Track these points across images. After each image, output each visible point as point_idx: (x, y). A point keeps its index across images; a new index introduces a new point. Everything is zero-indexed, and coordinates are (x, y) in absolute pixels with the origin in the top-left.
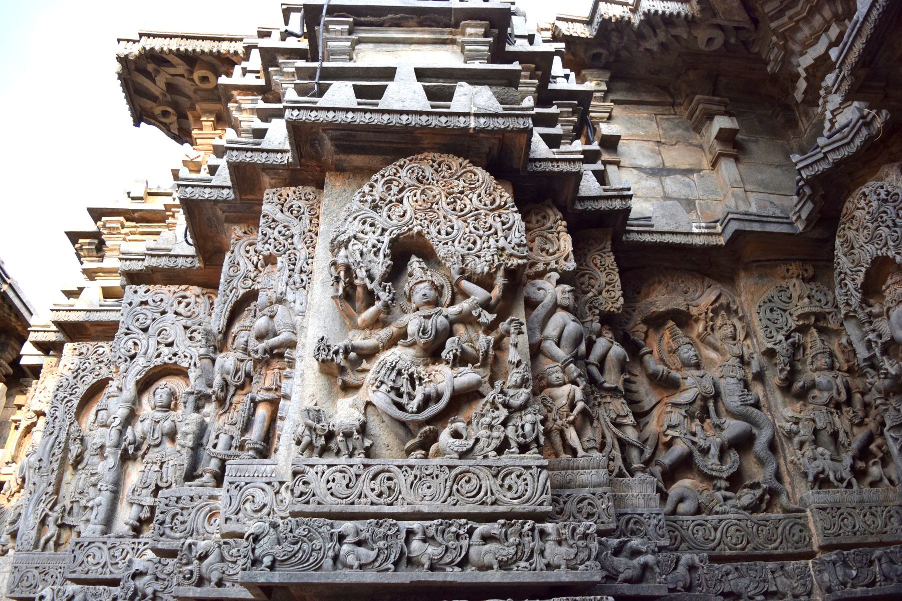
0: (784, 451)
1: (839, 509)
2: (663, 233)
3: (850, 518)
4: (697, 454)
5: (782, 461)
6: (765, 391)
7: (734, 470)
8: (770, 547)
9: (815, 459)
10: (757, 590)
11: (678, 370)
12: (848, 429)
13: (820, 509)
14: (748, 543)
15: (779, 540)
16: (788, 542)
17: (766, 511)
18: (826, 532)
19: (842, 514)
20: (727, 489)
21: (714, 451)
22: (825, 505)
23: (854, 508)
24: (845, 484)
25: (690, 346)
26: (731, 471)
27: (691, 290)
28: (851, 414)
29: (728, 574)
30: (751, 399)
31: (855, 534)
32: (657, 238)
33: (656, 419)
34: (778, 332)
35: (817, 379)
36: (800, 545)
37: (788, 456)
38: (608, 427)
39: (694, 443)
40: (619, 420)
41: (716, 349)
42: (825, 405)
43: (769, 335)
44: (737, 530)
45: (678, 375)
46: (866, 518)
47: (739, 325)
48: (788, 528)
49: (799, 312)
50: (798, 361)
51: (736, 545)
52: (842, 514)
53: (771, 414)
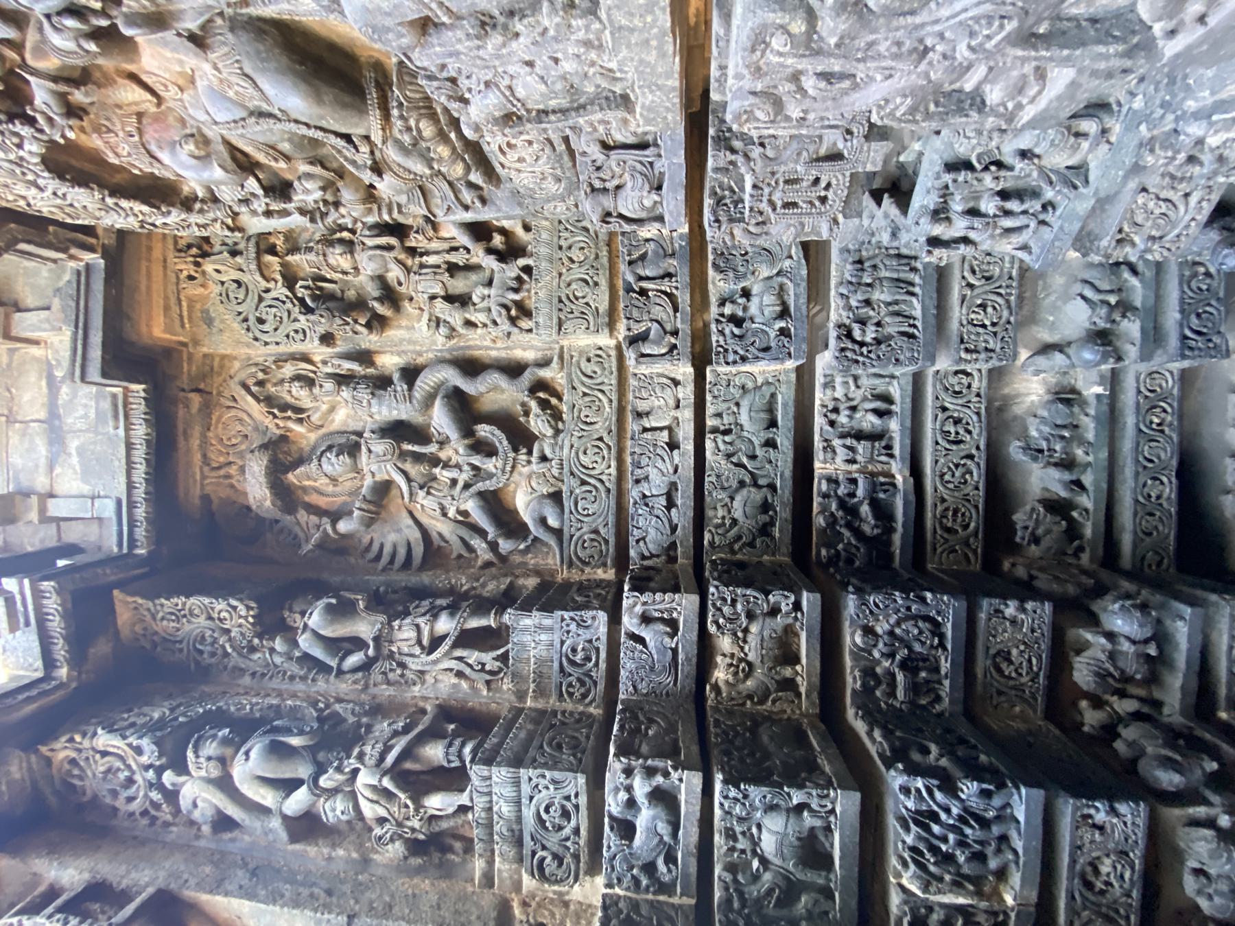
0: (480, 348)
1: (560, 301)
2: (130, 486)
3: (574, 286)
4: (481, 486)
5: (494, 354)
6: (392, 353)
7: (503, 436)
8: (608, 409)
9: (490, 310)
10: (666, 458)
11: (362, 479)
12: (446, 246)
13: (560, 329)
14: (601, 439)
15: (600, 395)
16: (602, 383)
17: (560, 399)
18: (592, 328)
19: (568, 298)
20: (530, 453)
21: (476, 460)
22: (555, 321)
23: (560, 275)
24: (525, 277)
25: (324, 459)
26: (505, 443)
27: (239, 428)
28: (420, 237)
29: (645, 496)
30: (401, 387)
31: (596, 284)
32: (140, 493)
33: (434, 522)
34: (296, 320)
35: (369, 273)
36: (606, 366)
37: (485, 343)
38: (435, 662)
39: (467, 486)
40: (425, 642)
41: (332, 409)
42: (409, 273)
43: (301, 336)
44: (585, 453)
45: (368, 481)
46: (575, 259)
47: (289, 370)
48: (585, 379)
49: (260, 279)
50: (343, 291)
51: (604, 458)
52: (568, 298)
53: (426, 352)
